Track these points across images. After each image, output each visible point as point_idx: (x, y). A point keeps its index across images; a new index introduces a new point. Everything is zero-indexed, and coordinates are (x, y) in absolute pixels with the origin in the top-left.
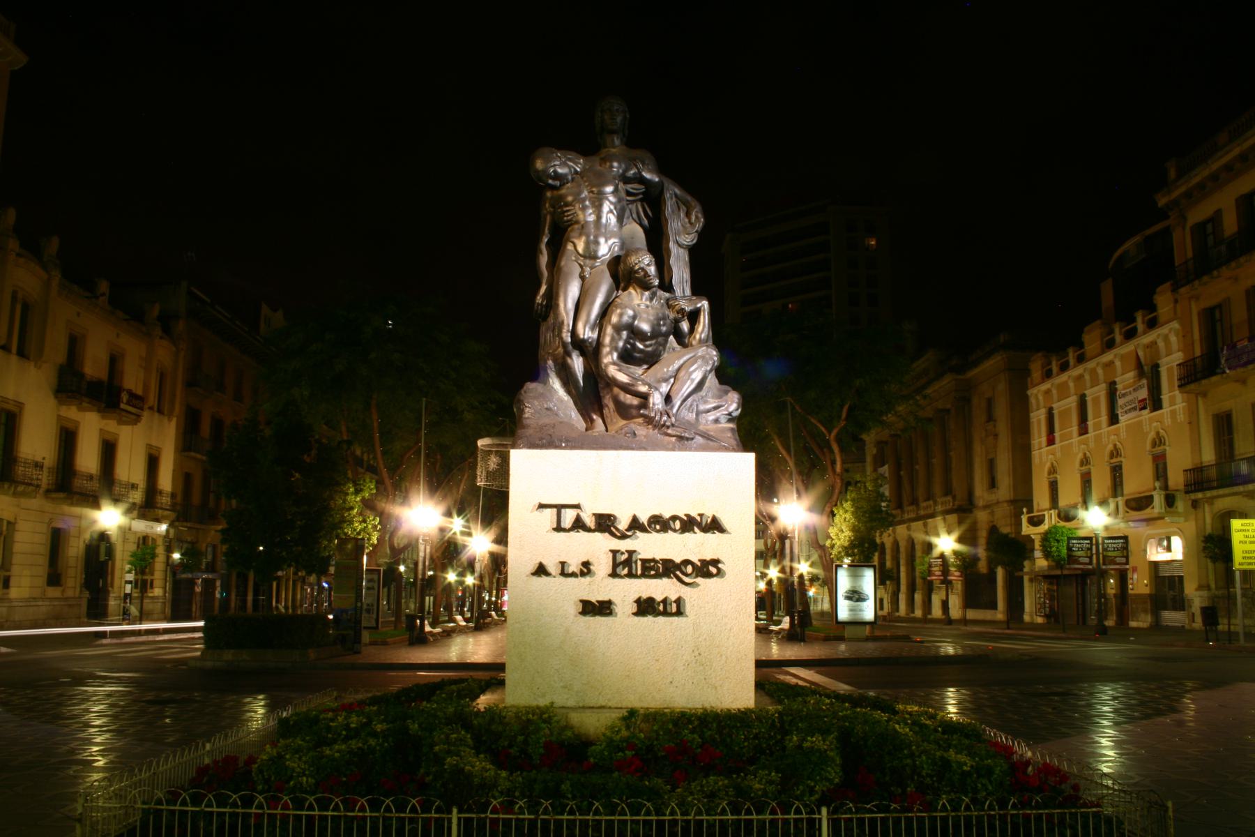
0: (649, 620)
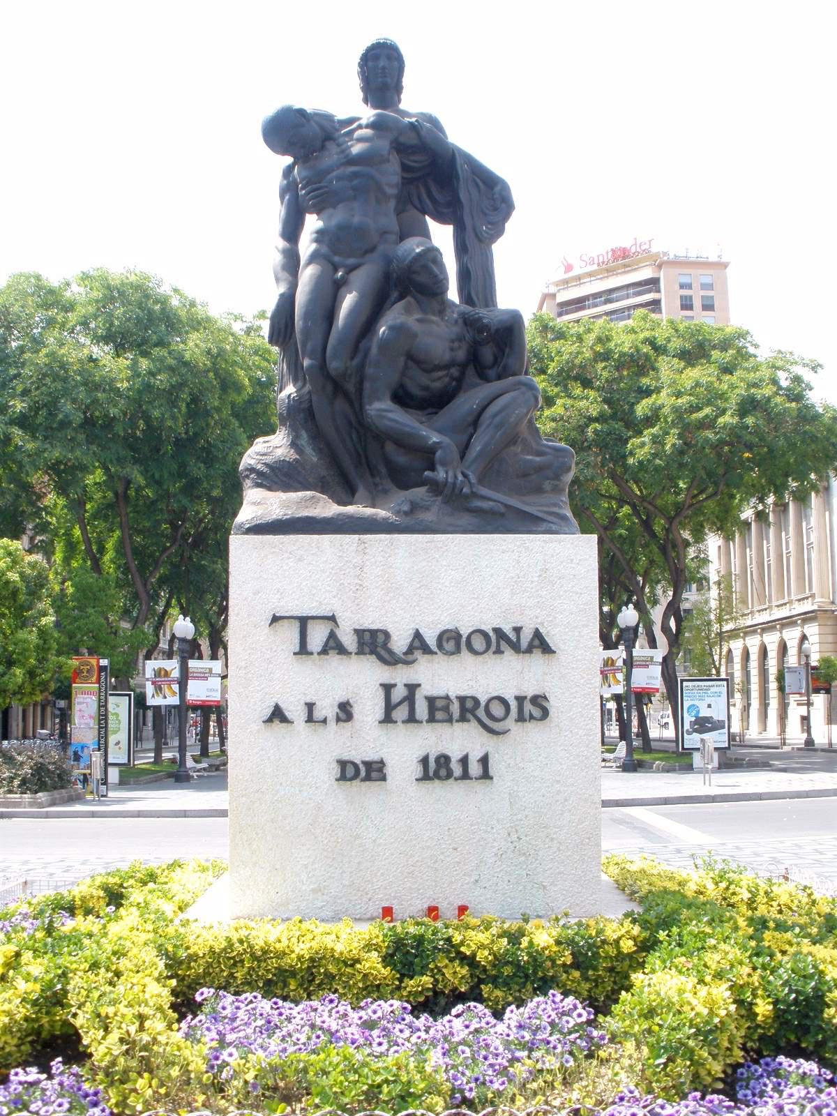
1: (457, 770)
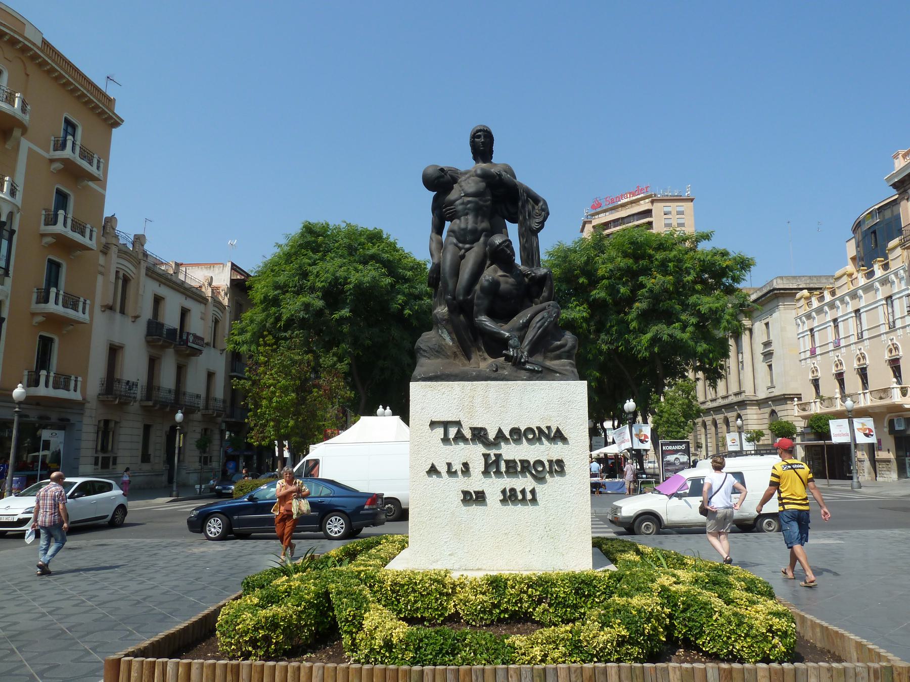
0: (510, 508)
1: (520, 497)
